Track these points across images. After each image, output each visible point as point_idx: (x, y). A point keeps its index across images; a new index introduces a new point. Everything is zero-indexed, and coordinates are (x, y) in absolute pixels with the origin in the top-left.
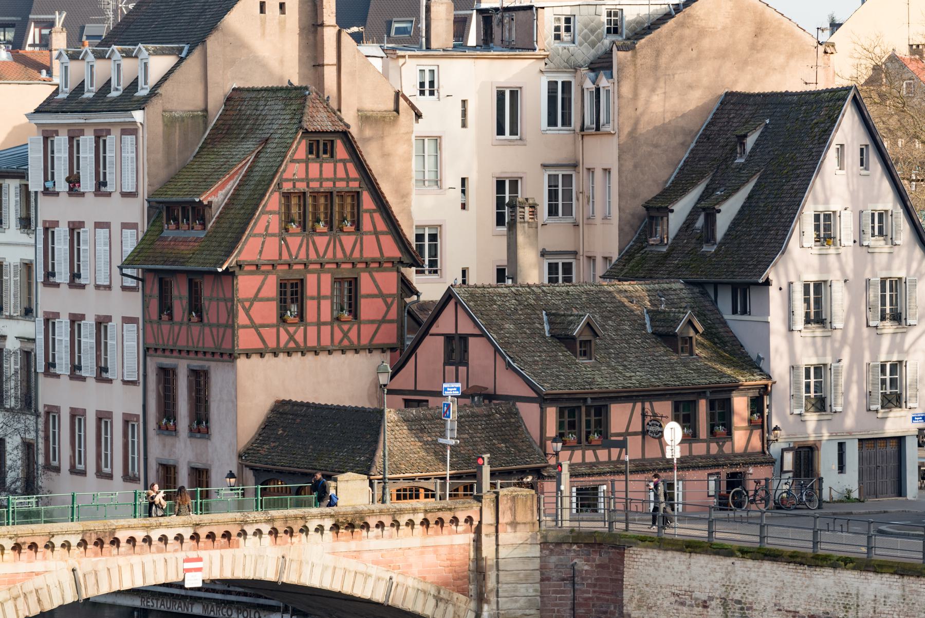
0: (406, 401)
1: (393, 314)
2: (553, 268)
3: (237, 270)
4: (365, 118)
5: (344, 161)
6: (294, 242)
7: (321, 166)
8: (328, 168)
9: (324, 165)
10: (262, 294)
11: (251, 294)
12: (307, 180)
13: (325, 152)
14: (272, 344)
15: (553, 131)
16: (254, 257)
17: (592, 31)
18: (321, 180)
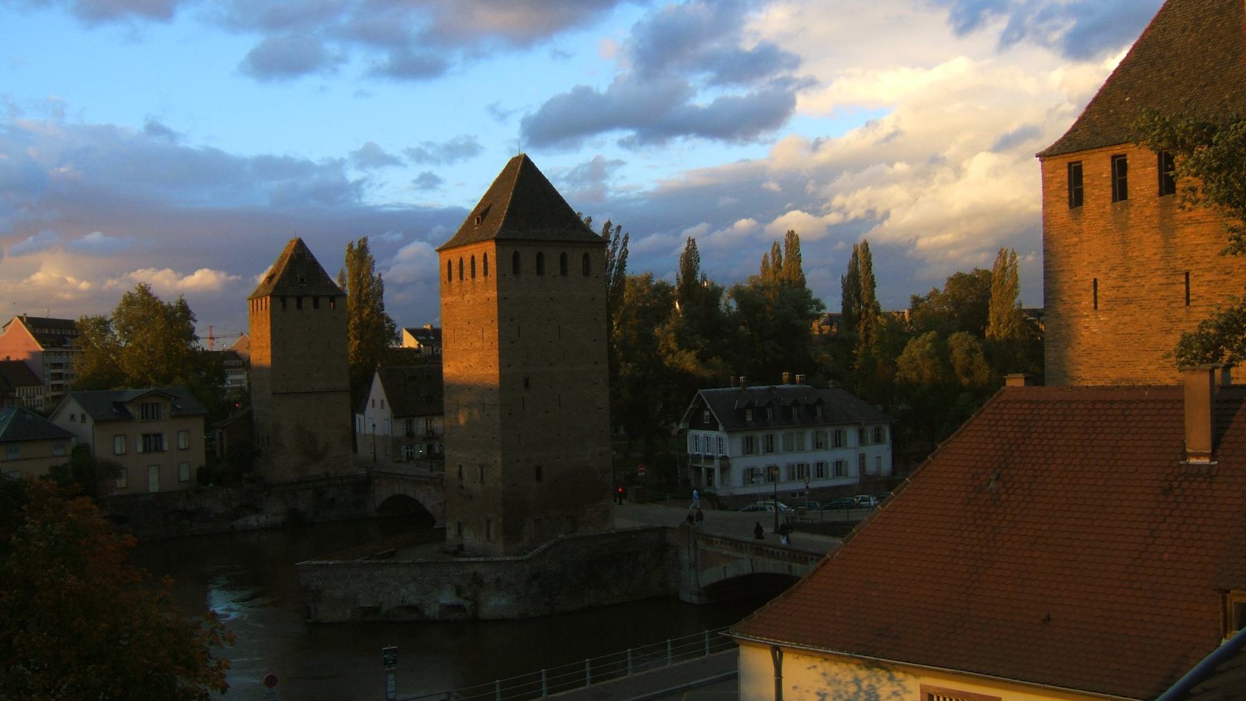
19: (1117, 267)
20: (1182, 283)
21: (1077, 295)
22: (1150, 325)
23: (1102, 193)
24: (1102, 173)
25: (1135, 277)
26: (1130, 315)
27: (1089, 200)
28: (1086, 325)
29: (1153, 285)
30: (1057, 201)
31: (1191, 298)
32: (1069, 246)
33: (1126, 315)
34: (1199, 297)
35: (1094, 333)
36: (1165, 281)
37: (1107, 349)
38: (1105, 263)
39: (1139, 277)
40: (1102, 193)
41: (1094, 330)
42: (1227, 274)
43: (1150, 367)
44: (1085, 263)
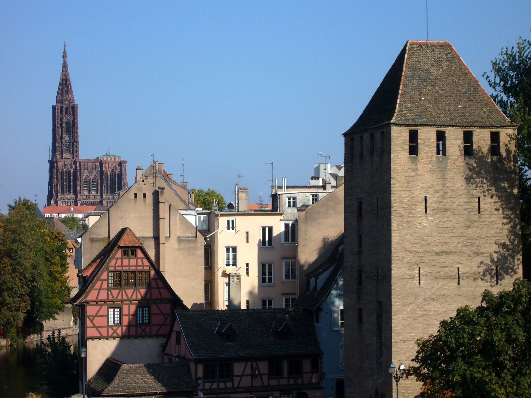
0: (169, 358)
1: (169, 321)
2: (287, 300)
3: (86, 304)
4: (180, 240)
5: (142, 259)
6: (115, 292)
7: (129, 261)
8: (133, 262)
9: (131, 260)
10: (100, 313)
11: (94, 314)
12: (122, 266)
13: (132, 254)
14: (105, 334)
15: (286, 244)
16: (94, 298)
18: (129, 266)
19: (439, 191)
20: (476, 202)
21: (413, 205)
22: (459, 223)
24: (431, 139)
25: (450, 197)
26: (447, 217)
27: (422, 153)
28: (420, 222)
29: (460, 202)
30: (401, 151)
31: (481, 210)
32: (409, 177)
33: (444, 217)
34: (486, 210)
35: (425, 226)
36: (467, 201)
37: (433, 235)
38: (432, 188)
39: (453, 197)
40: (430, 150)
41: (425, 225)
43: (458, 245)
44: (419, 187)
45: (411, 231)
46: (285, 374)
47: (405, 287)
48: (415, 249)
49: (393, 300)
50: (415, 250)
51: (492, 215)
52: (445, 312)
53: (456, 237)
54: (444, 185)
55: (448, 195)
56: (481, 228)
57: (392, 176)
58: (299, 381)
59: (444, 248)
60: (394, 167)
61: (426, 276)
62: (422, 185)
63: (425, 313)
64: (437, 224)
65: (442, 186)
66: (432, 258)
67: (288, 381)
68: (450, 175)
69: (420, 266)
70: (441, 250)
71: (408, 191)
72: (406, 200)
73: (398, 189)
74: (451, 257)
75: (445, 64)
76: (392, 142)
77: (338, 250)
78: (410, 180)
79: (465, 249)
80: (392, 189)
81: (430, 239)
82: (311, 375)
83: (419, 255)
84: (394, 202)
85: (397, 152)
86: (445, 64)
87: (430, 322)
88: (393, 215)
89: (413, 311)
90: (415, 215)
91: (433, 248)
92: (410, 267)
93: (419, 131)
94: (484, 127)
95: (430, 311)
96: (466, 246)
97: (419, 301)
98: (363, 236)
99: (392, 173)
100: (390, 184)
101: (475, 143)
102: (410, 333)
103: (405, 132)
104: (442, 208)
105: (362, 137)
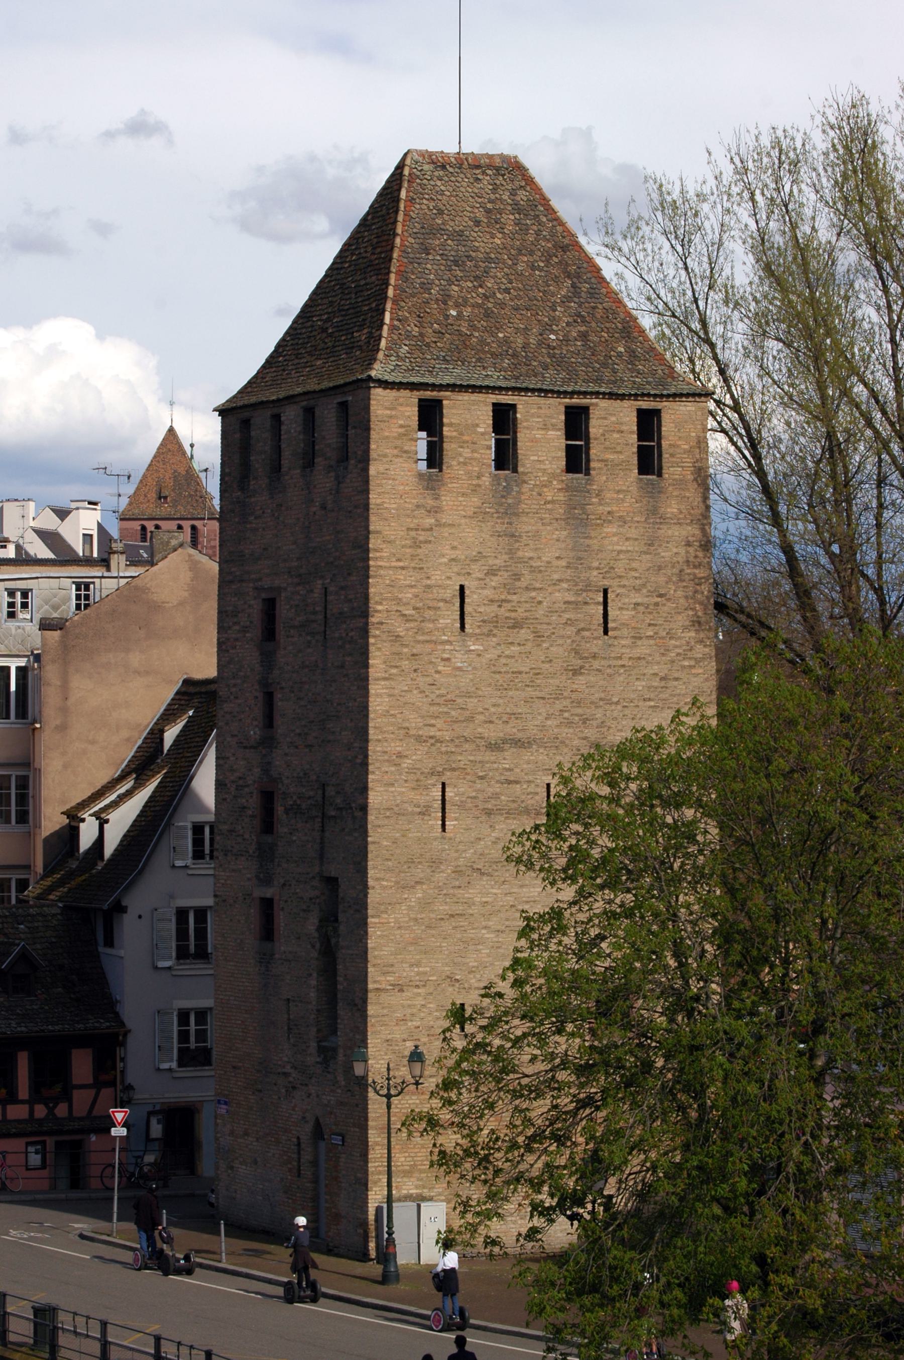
17: (55, 608)
19: (499, 570)
20: (598, 603)
21: (429, 608)
22: (551, 661)
23: (476, 455)
24: (477, 425)
26: (519, 644)
27: (454, 463)
28: (446, 656)
32: (417, 530)
33: (512, 643)
37: (480, 693)
39: (535, 589)
40: (476, 455)
41: (459, 665)
42: (661, 596)
43: (549, 723)
44: (445, 560)
45: (421, 681)
46: (23, 1092)
47: (403, 836)
48: (432, 732)
49: (371, 873)
50: (432, 734)
51: (640, 638)
52: (512, 906)
53: (543, 698)
54: (511, 552)
55: (523, 583)
56: (610, 675)
57: (372, 528)
58: (61, 1110)
59: (511, 729)
60: (379, 501)
61: (461, 806)
62: (453, 554)
63: (459, 908)
64: (492, 663)
65: (506, 557)
66: (479, 758)
67: (32, 1112)
68: (526, 525)
69: (443, 779)
70: (501, 735)
71: (415, 568)
72: (410, 596)
73: (387, 564)
74: (527, 755)
75: (509, 219)
76: (372, 432)
77: (162, 740)
78: (421, 538)
79: (565, 732)
80: (371, 563)
81: (472, 703)
82: (93, 1092)
83: (443, 749)
84: (377, 599)
85: (385, 460)
86: (509, 219)
87: (471, 933)
88: (375, 637)
89: (426, 904)
90: (434, 638)
91: (480, 730)
92: (417, 781)
93: (445, 402)
94: (622, 397)
95: (469, 903)
96: (569, 724)
97: (440, 877)
98: (278, 696)
99: (372, 518)
100: (367, 550)
101: (596, 439)
102: (418, 964)
103: (407, 405)
104: (507, 618)
105: (277, 418)
